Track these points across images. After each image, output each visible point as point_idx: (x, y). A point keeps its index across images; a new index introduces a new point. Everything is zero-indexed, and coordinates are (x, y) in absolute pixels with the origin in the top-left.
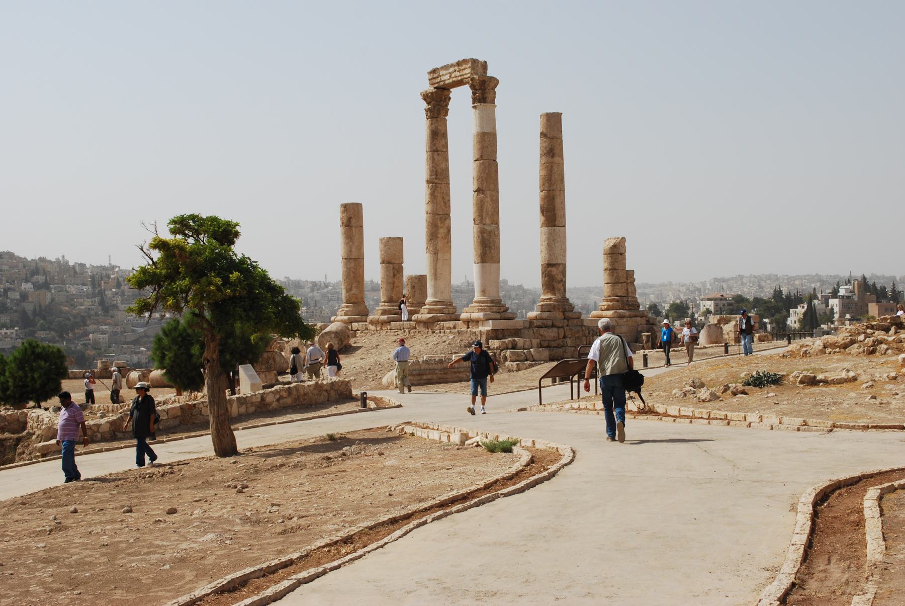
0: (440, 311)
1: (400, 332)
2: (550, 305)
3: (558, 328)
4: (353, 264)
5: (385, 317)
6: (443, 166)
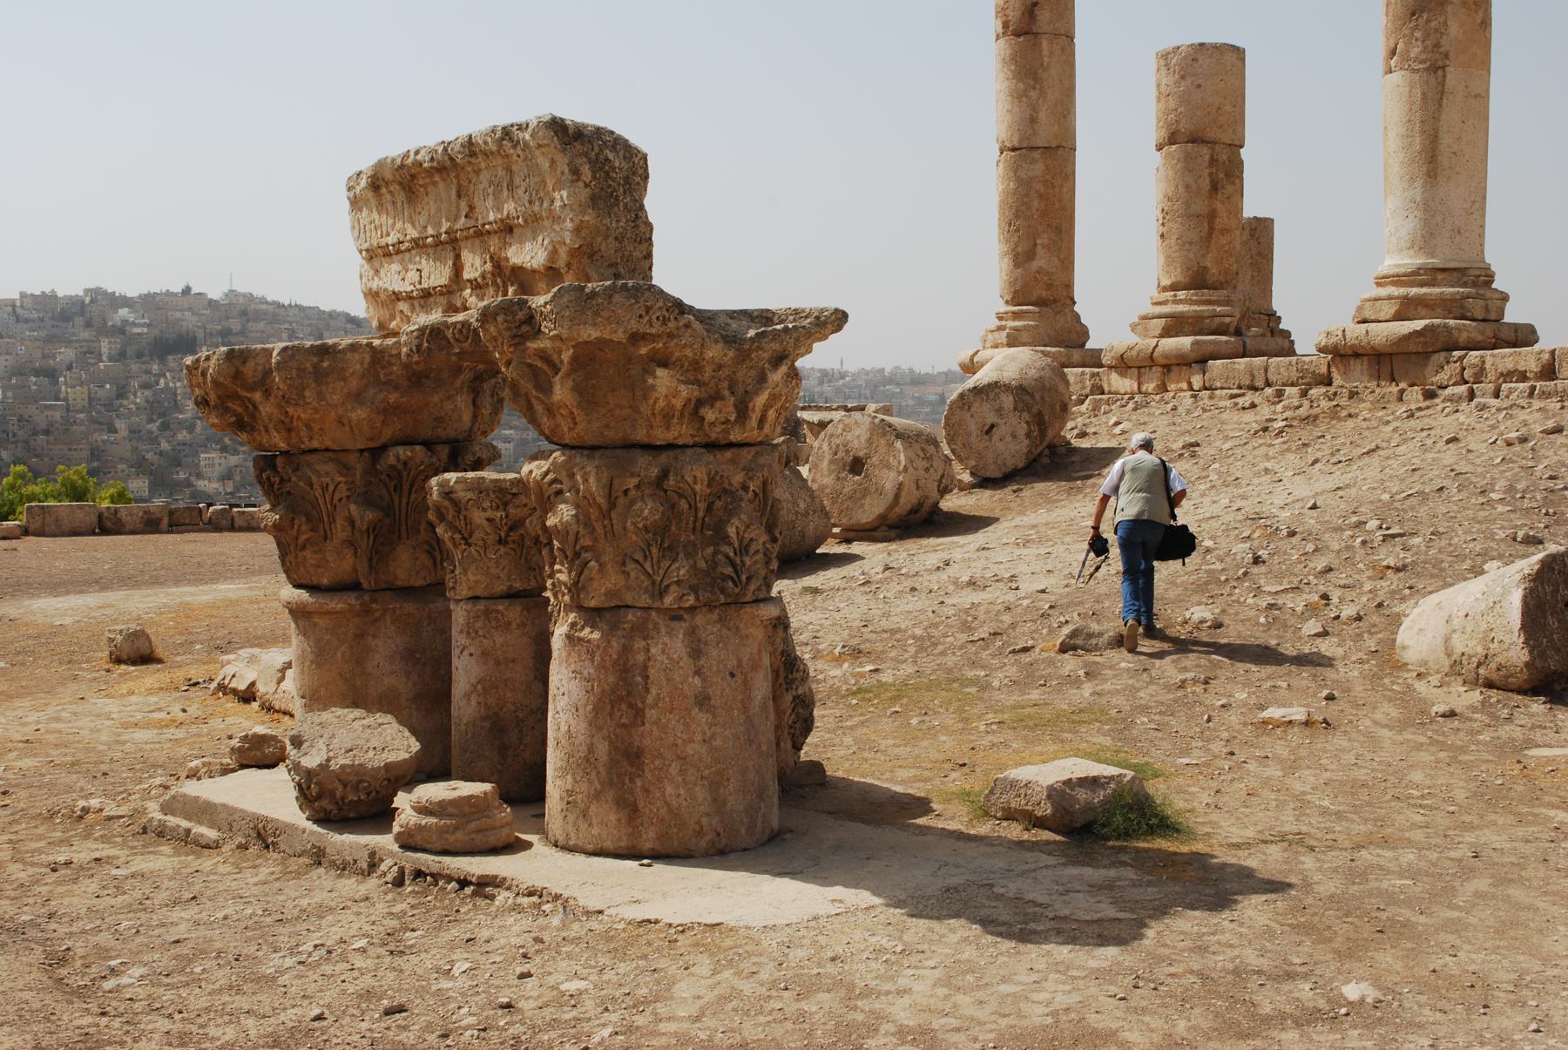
1: (1256, 397)
4: (1039, 168)
5: (1184, 342)
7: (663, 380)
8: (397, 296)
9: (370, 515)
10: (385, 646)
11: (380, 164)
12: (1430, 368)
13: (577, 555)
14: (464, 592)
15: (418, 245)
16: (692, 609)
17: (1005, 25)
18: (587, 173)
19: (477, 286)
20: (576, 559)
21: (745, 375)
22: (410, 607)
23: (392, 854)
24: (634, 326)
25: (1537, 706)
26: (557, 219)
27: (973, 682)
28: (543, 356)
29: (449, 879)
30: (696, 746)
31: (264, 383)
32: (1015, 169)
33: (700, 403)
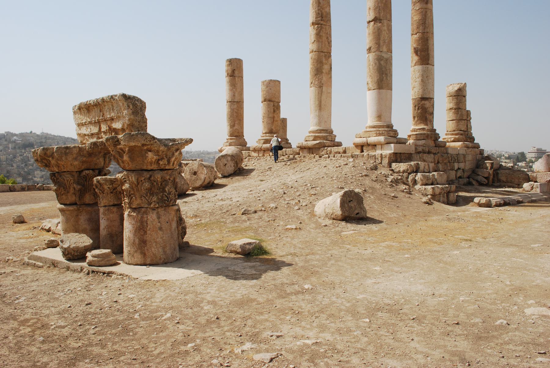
0: (325, 138)
2: (424, 134)
3: (434, 154)
4: (236, 106)
6: (327, 10)
7: (150, 155)
8: (85, 135)
9: (79, 187)
10: (83, 219)
11: (81, 104)
12: (320, 151)
13: (130, 196)
14: (102, 205)
15: (90, 123)
16: (158, 207)
17: (228, 74)
18: (131, 107)
19: (105, 133)
20: (130, 196)
21: (170, 154)
22: (89, 208)
23: (86, 267)
24: (143, 142)
25: (343, 223)
26: (124, 117)
27: (222, 222)
28: (121, 149)
29: (101, 272)
30: (159, 240)
31: (52, 155)
32: (230, 106)
33: (159, 160)
